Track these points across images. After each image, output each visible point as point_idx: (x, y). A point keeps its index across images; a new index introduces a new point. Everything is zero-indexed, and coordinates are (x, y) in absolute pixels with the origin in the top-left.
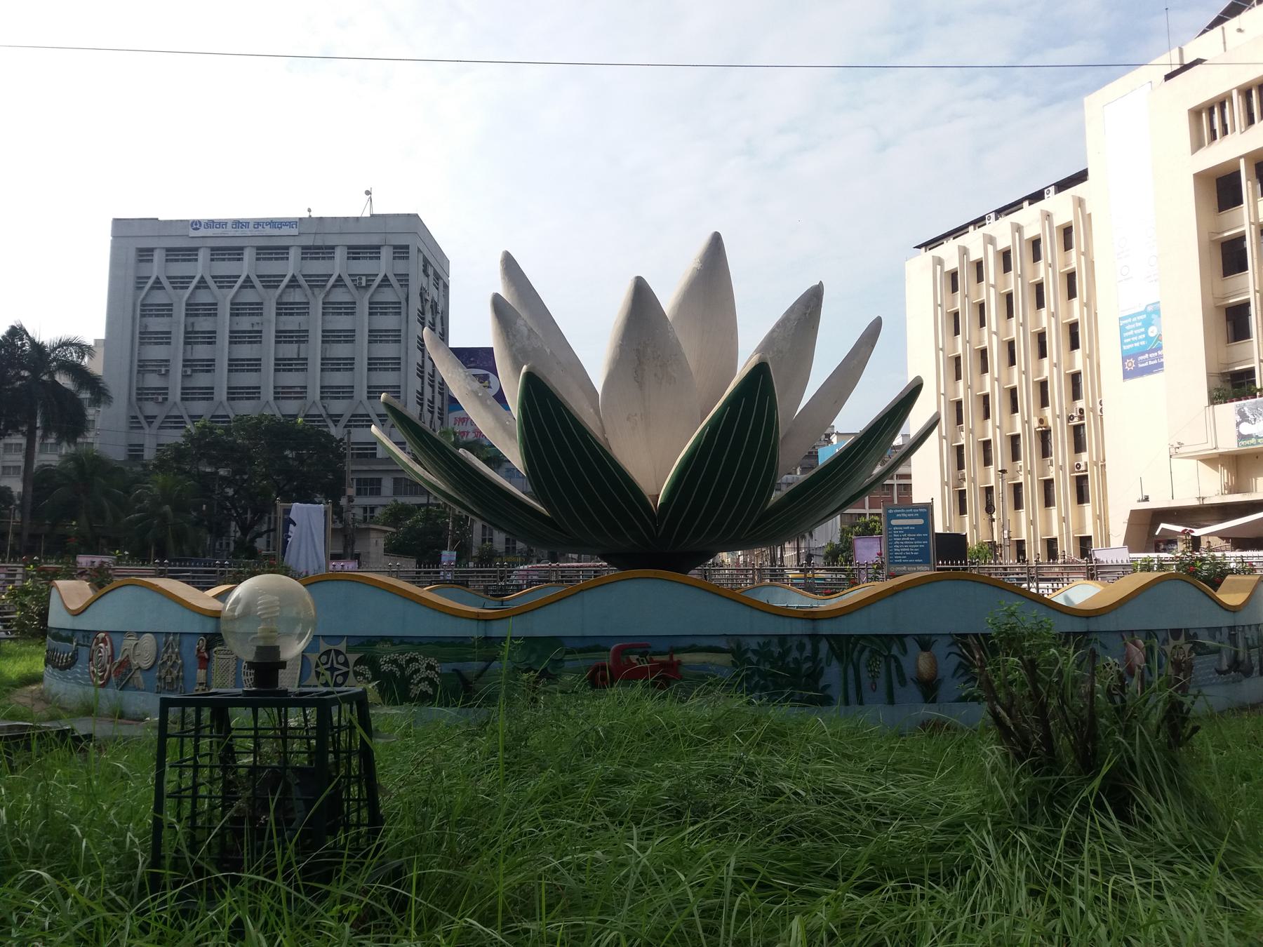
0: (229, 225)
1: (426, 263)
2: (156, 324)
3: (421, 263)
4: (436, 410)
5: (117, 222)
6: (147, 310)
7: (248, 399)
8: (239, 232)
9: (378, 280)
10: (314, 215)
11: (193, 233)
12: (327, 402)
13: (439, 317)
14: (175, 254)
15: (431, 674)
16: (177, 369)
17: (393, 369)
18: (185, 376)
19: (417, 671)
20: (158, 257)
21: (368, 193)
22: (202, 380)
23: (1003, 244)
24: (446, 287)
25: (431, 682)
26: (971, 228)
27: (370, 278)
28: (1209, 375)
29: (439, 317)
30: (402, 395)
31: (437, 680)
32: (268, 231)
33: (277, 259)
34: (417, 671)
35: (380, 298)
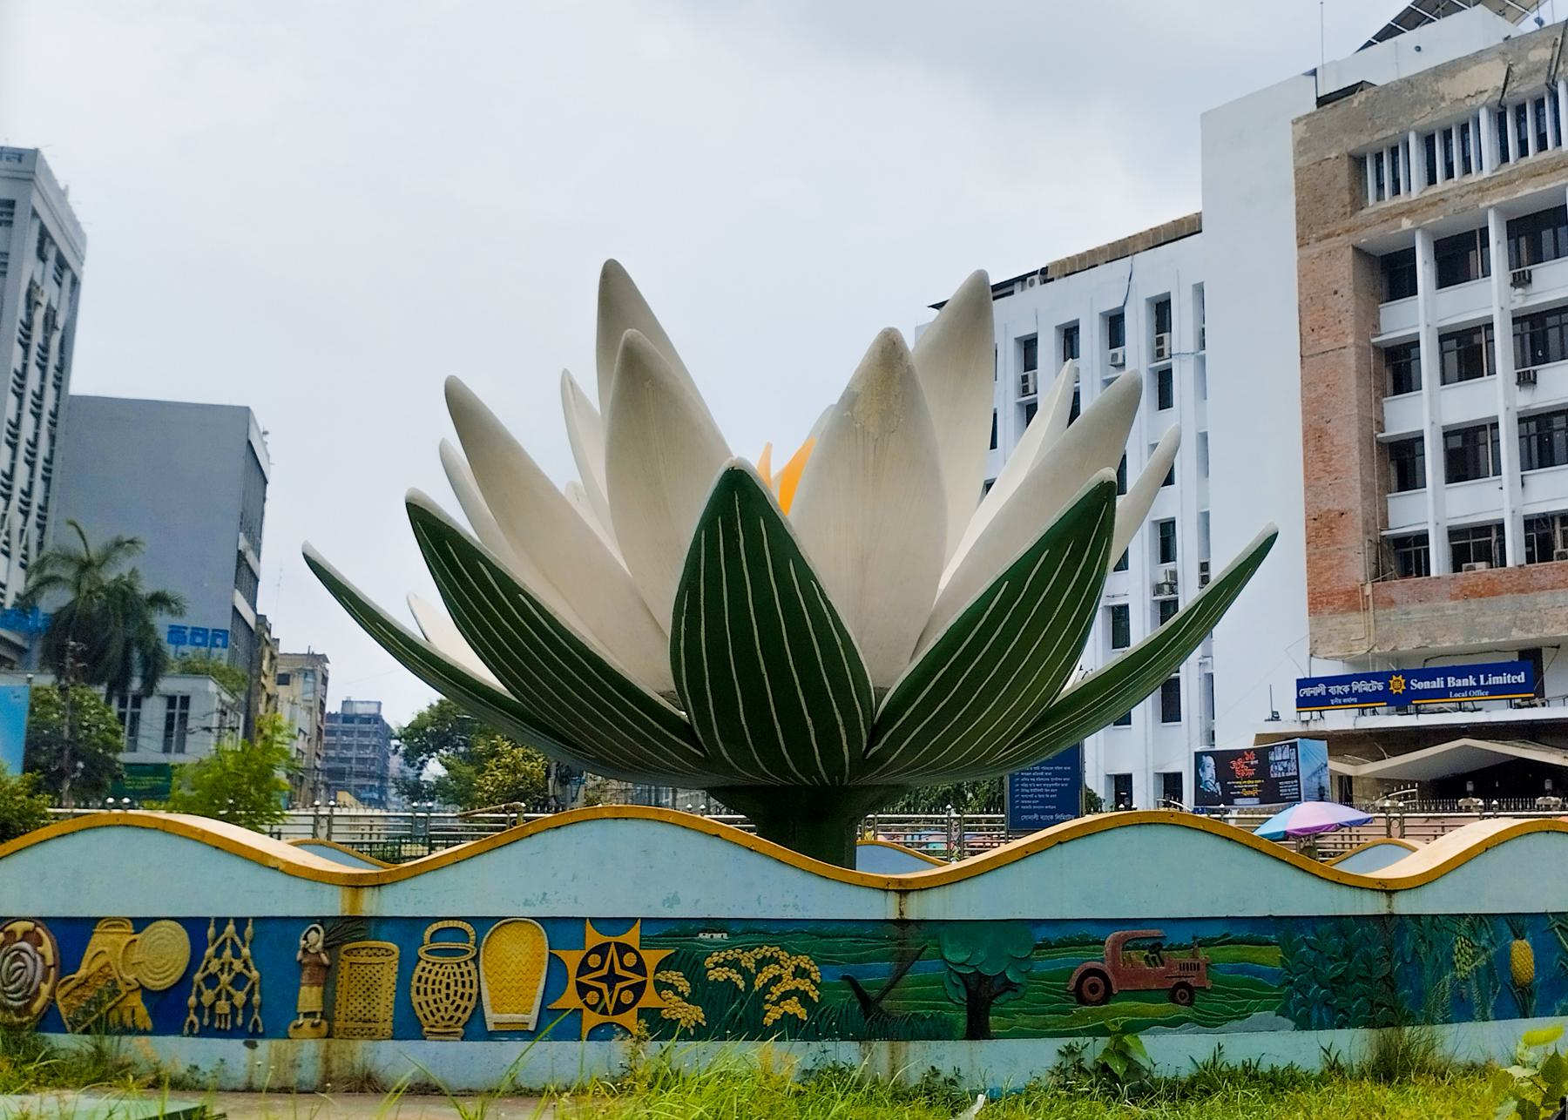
1: (44, 235)
4: (34, 510)
15: (804, 985)
19: (777, 979)
24: (75, 282)
25: (804, 998)
26: (1017, 287)
31: (815, 995)
34: (777, 979)
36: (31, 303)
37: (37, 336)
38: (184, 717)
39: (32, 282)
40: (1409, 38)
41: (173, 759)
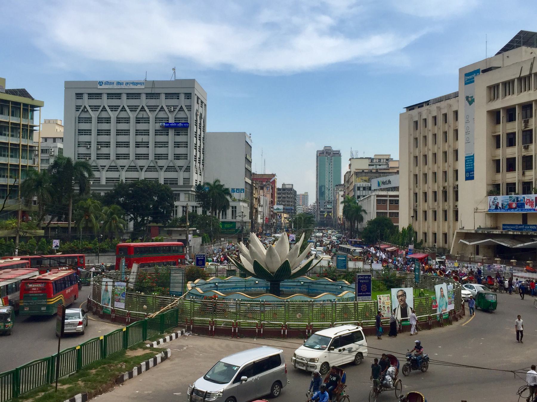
0: (115, 84)
1: (198, 98)
2: (84, 126)
3: (196, 99)
5: (67, 83)
6: (80, 120)
7: (124, 159)
8: (119, 87)
9: (178, 108)
10: (150, 79)
11: (99, 87)
12: (157, 160)
13: (202, 120)
14: (91, 96)
16: (94, 145)
17: (185, 147)
18: (98, 149)
20: (86, 97)
21: (174, 69)
22: (104, 151)
23: (434, 114)
24: (205, 105)
27: (175, 107)
28: (488, 185)
29: (202, 120)
30: (188, 158)
32: (132, 86)
33: (135, 99)
35: (178, 116)
36: (197, 115)
37: (199, 122)
38: (235, 211)
39: (197, 110)
40: (506, 54)
41: (234, 220)
